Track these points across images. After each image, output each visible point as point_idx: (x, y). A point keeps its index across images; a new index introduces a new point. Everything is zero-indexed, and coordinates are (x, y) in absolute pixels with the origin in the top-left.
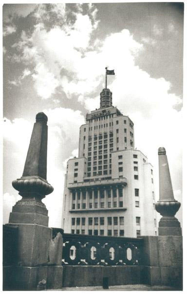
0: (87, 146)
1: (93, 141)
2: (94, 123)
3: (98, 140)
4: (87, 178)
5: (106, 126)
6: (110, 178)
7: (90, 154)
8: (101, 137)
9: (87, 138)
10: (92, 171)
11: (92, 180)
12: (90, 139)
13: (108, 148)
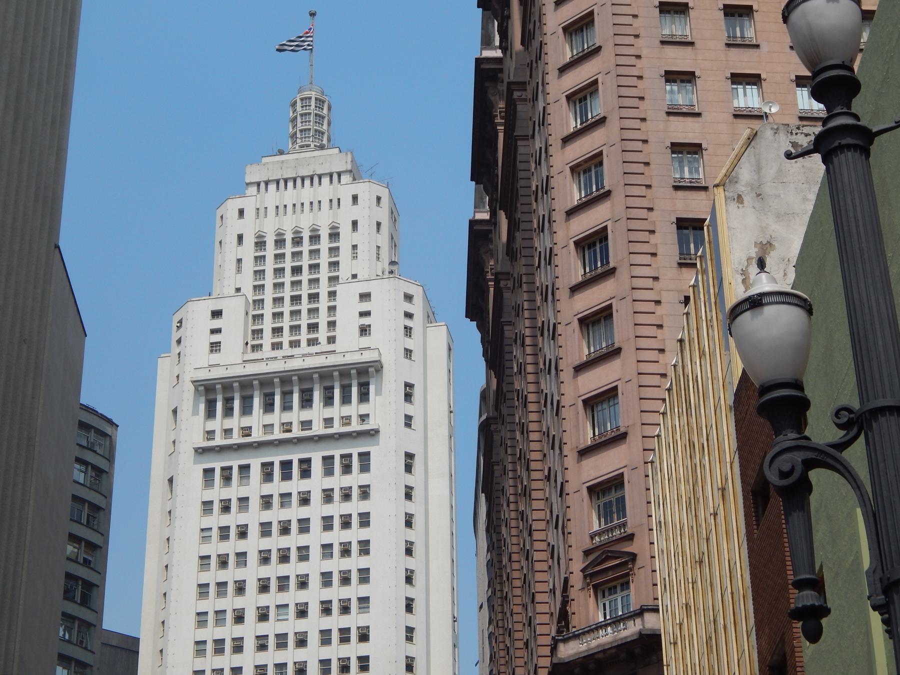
0: (249, 266)
1: (270, 251)
3: (289, 249)
5: (316, 205)
7: (259, 288)
8: (297, 241)
9: (249, 241)
10: (268, 339)
12: (260, 244)
13: (324, 274)
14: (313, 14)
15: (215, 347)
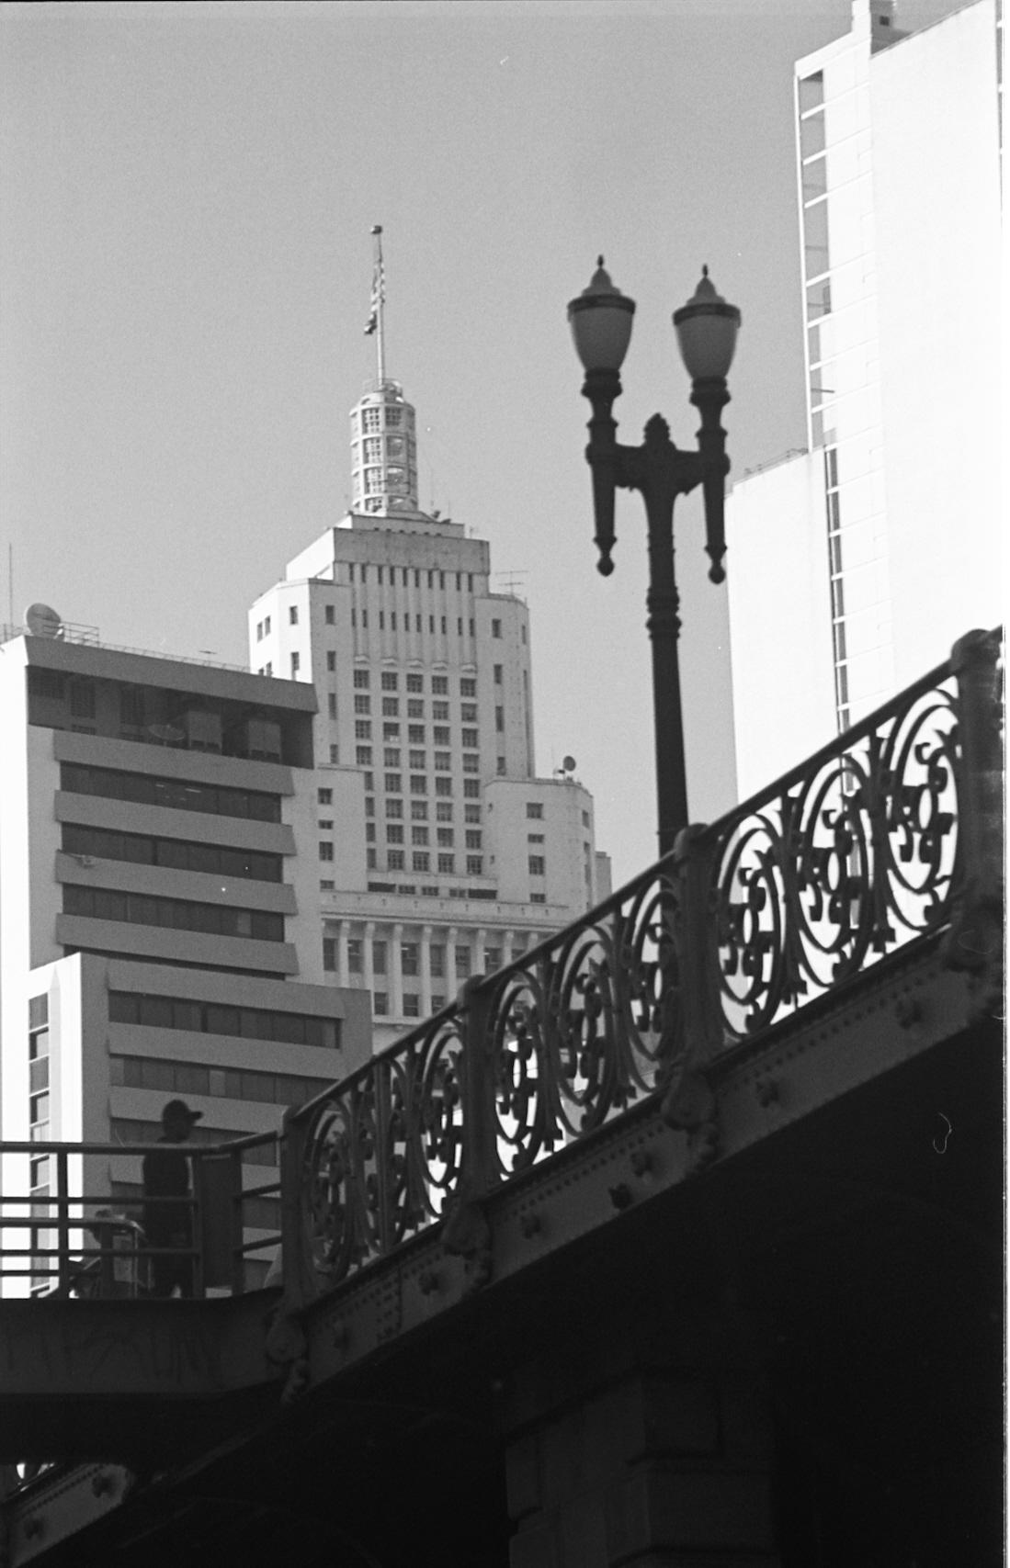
1: (376, 692)
2: (376, 595)
4: (377, 878)
6: (490, 895)
11: (409, 890)
12: (361, 678)
14: (378, 230)
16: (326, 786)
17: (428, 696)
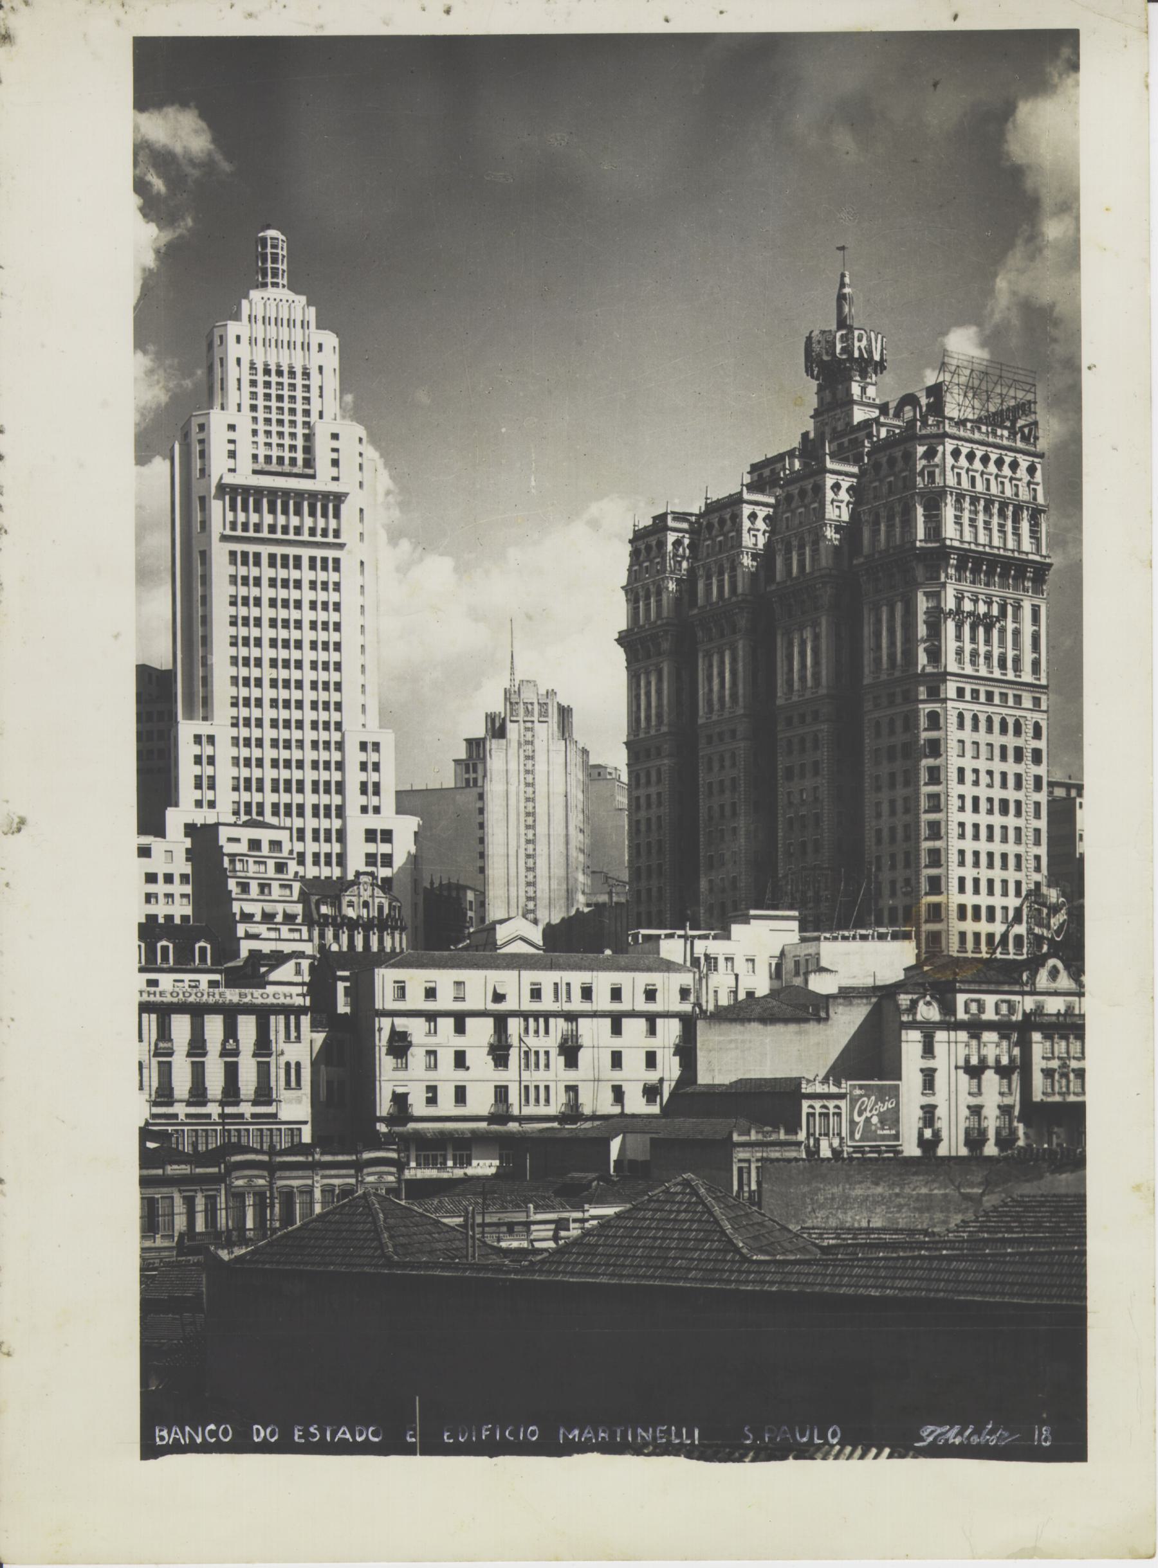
1: (261, 378)
9: (245, 365)
15: (232, 454)
16: (232, 423)
17: (286, 380)
